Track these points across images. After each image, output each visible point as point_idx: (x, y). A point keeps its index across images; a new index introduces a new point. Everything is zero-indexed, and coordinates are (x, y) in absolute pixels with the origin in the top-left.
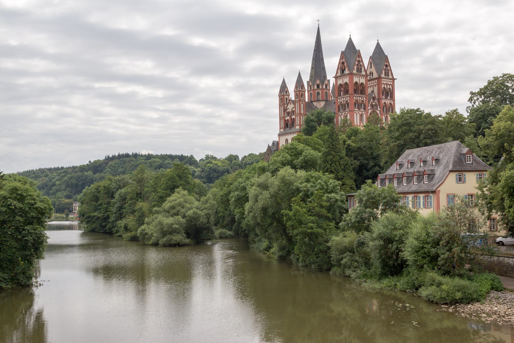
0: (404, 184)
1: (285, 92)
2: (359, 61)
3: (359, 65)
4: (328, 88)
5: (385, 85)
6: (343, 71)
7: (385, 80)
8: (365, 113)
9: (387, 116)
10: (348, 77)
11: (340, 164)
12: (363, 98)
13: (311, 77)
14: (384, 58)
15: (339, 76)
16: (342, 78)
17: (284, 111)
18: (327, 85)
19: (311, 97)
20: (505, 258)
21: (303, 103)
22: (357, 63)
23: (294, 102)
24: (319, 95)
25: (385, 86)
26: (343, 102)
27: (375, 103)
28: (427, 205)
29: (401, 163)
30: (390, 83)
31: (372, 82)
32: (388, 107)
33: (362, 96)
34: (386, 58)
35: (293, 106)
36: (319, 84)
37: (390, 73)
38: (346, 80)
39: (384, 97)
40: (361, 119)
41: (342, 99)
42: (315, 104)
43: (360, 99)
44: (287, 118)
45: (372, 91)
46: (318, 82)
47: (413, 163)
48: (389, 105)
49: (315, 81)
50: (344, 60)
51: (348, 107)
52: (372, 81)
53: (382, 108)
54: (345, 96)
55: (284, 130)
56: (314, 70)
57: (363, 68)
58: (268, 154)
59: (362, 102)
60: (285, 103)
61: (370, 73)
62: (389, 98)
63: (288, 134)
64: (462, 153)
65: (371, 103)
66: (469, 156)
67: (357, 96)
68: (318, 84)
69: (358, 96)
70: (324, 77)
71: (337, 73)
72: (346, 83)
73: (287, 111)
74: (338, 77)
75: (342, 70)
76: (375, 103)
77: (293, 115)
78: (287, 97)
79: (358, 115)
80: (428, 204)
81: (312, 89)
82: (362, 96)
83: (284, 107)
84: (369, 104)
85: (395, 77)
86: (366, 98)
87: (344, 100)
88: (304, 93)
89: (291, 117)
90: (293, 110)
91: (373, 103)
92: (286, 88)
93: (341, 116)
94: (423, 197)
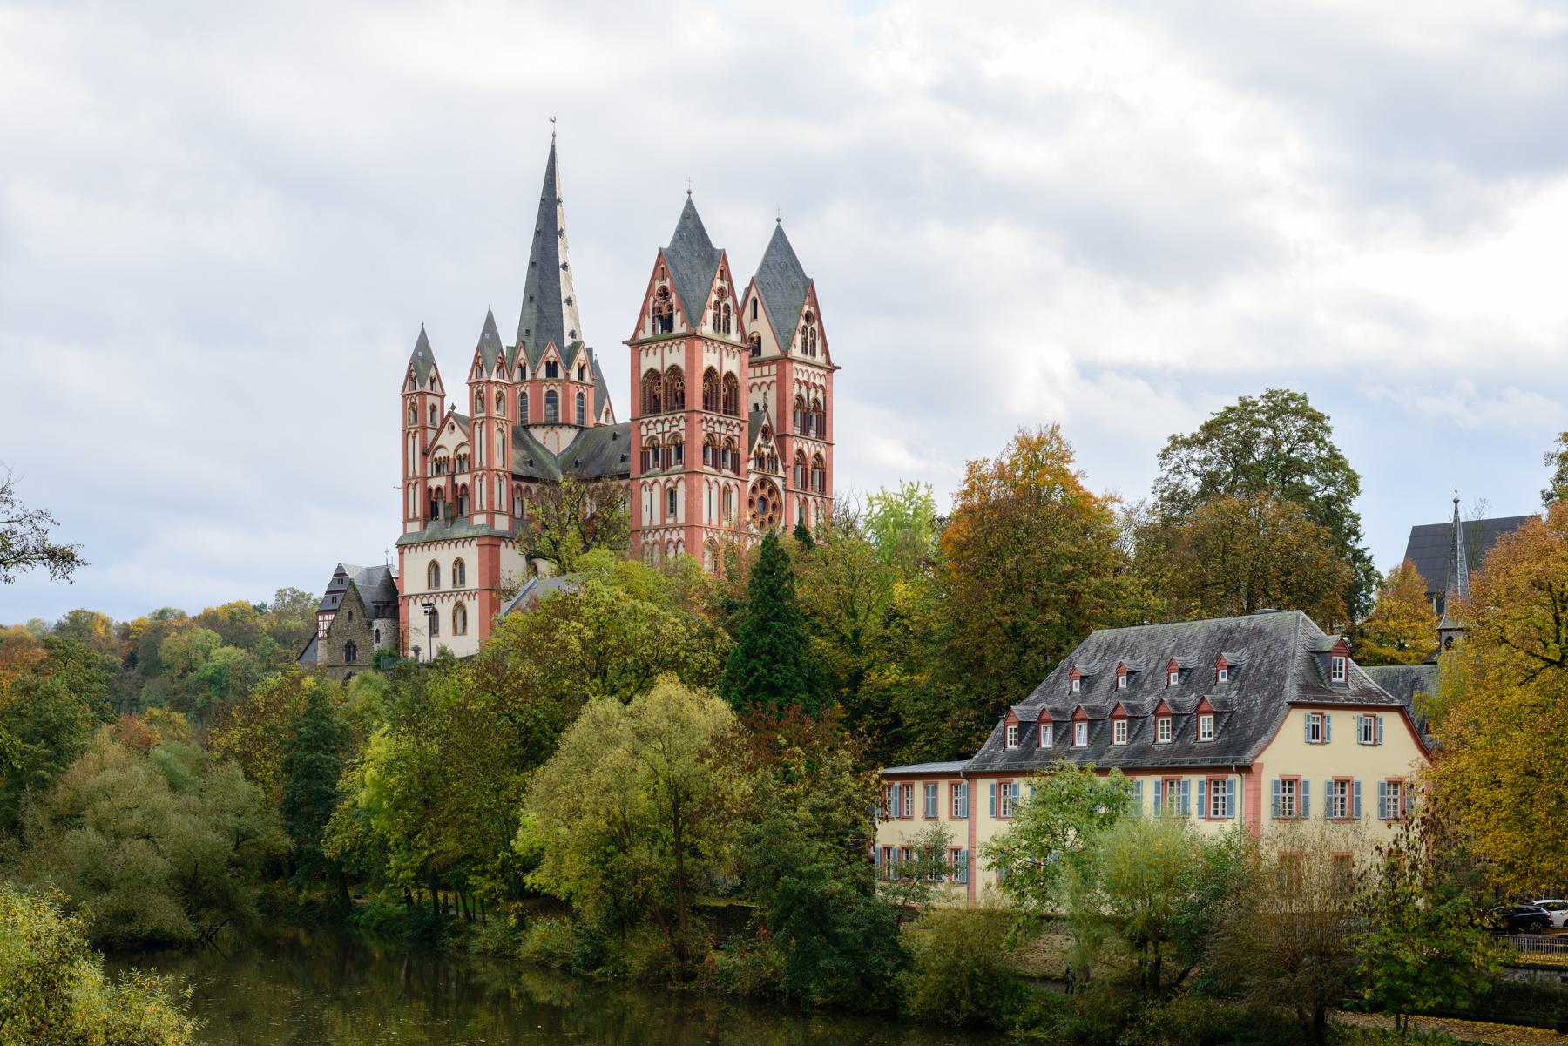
0: (1116, 742)
1: (428, 382)
3: (722, 305)
5: (804, 387)
6: (667, 323)
7: (804, 368)
9: (805, 501)
10: (683, 347)
11: (797, 664)
12: (731, 427)
13: (525, 332)
14: (801, 287)
16: (659, 350)
17: (425, 454)
19: (524, 407)
21: (500, 430)
22: (714, 298)
23: (468, 423)
26: (660, 437)
27: (769, 450)
28: (1212, 809)
29: (1087, 674)
31: (758, 374)
32: (810, 468)
33: (728, 421)
34: (809, 286)
35: (464, 439)
36: (555, 363)
37: (819, 343)
38: (675, 356)
39: (797, 432)
41: (659, 426)
42: (538, 434)
43: (723, 431)
44: (434, 483)
45: (756, 406)
47: (1134, 673)
48: (814, 460)
49: (540, 349)
51: (679, 455)
52: (758, 370)
54: (670, 417)
56: (534, 305)
57: (733, 320)
59: (726, 443)
60: (429, 424)
62: (813, 434)
63: (439, 542)
64: (1317, 650)
65: (756, 448)
66: (1338, 658)
67: (712, 419)
68: (551, 360)
71: (640, 326)
72: (675, 369)
74: (642, 343)
75: (661, 317)
76: (769, 450)
77: (462, 472)
78: (437, 401)
79: (715, 487)
81: (529, 376)
82: (728, 421)
83: (424, 439)
84: (749, 453)
86: (741, 429)
89: (453, 479)
90: (464, 450)
91: (764, 449)
92: (433, 367)
93: (651, 490)
94: (1201, 783)
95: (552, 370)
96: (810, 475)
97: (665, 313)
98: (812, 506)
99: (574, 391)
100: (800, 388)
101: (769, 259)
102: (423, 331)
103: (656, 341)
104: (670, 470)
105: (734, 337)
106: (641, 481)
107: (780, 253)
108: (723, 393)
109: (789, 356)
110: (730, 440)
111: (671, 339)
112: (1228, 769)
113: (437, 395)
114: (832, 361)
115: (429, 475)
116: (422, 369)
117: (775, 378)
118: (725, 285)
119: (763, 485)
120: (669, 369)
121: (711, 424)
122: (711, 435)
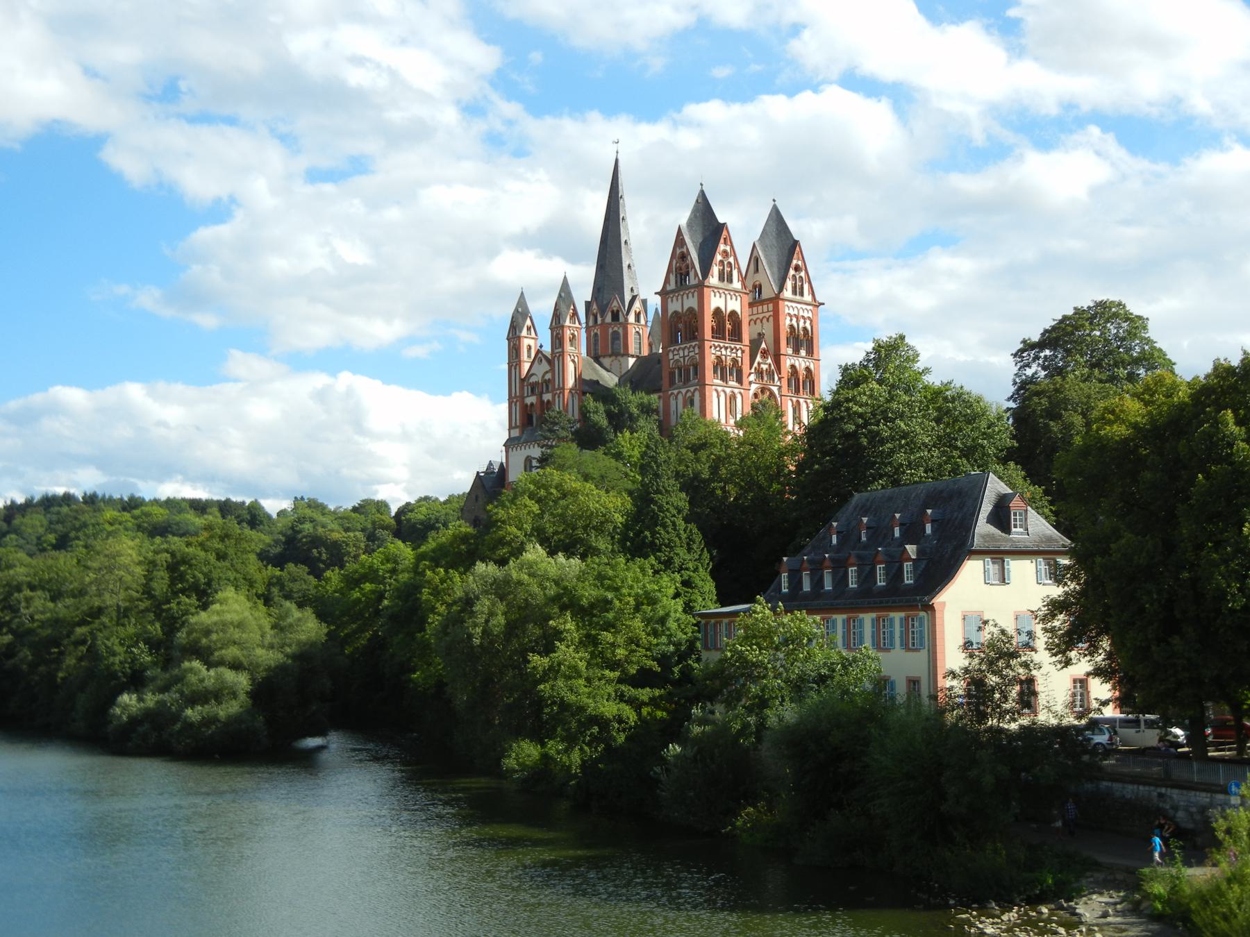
2: (725, 252)
3: (726, 263)
4: (643, 322)
5: (794, 319)
7: (794, 305)
8: (740, 393)
9: (798, 402)
12: (734, 351)
13: (598, 289)
15: (672, 291)
16: (680, 297)
18: (639, 313)
19: (596, 344)
20: (1115, 785)
21: (573, 361)
24: (618, 338)
25: (794, 322)
30: (806, 315)
31: (760, 311)
32: (801, 378)
33: (733, 346)
36: (618, 311)
37: (806, 287)
38: (691, 302)
39: (790, 351)
40: (731, 410)
43: (729, 353)
45: (759, 334)
46: (615, 303)
50: (685, 250)
51: (696, 373)
52: (760, 308)
53: (785, 383)
54: (688, 345)
55: (522, 432)
57: (735, 273)
58: (477, 497)
61: (755, 287)
62: (803, 353)
63: (531, 442)
65: (756, 365)
68: (615, 309)
69: (722, 345)
70: (632, 290)
71: (667, 281)
72: (691, 310)
73: (531, 381)
75: (681, 274)
77: (548, 391)
78: (532, 342)
80: (913, 638)
82: (733, 346)
84: (751, 369)
85: (819, 299)
86: (743, 352)
87: (686, 354)
88: (576, 333)
89: (541, 397)
90: (548, 376)
91: (762, 366)
92: (529, 319)
94: (901, 619)
95: (615, 316)
96: (801, 384)
97: (683, 271)
98: (804, 406)
99: (632, 331)
100: (791, 320)
101: (767, 228)
102: (522, 293)
103: (677, 292)
104: (690, 383)
105: (737, 285)
106: (670, 392)
107: (777, 222)
108: (728, 327)
109: (781, 297)
110: (735, 361)
111: (688, 289)
112: (914, 607)
113: (533, 338)
114: (817, 299)
115: (526, 395)
116: (519, 320)
117: (771, 313)
118: (728, 248)
119: (763, 390)
120: (687, 310)
121: (718, 349)
122: (718, 358)
